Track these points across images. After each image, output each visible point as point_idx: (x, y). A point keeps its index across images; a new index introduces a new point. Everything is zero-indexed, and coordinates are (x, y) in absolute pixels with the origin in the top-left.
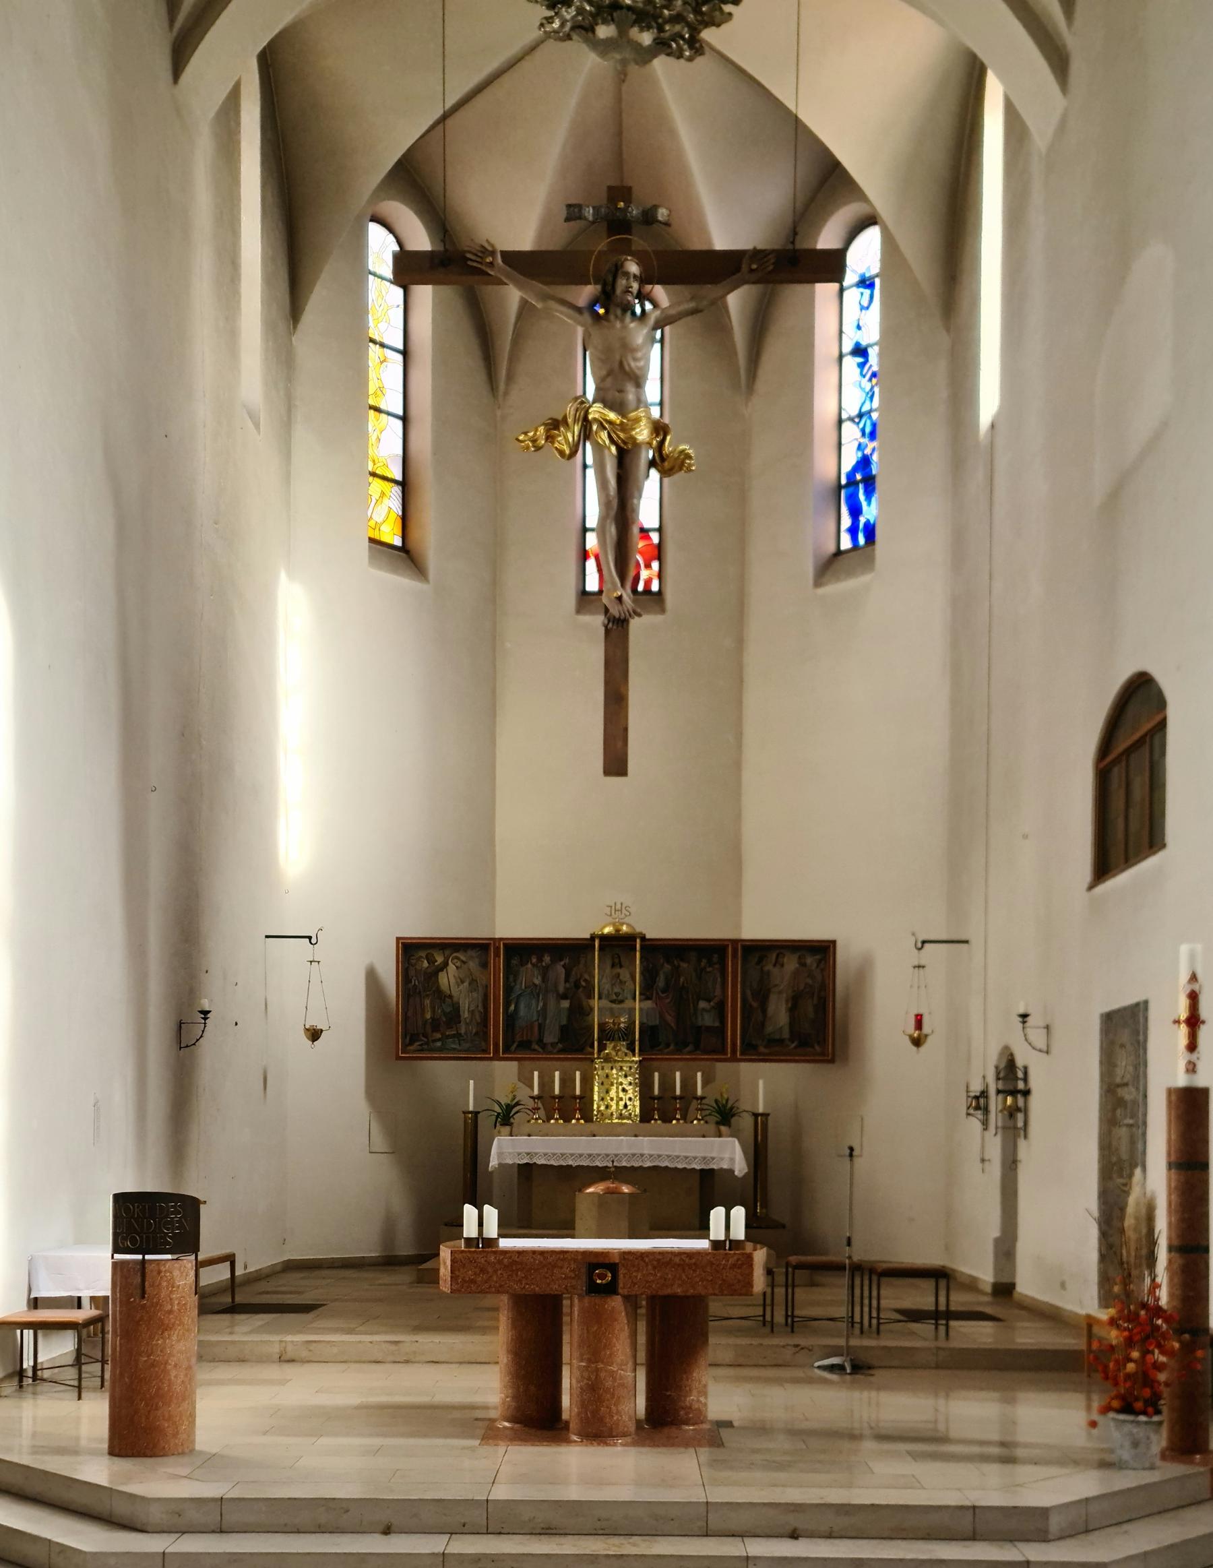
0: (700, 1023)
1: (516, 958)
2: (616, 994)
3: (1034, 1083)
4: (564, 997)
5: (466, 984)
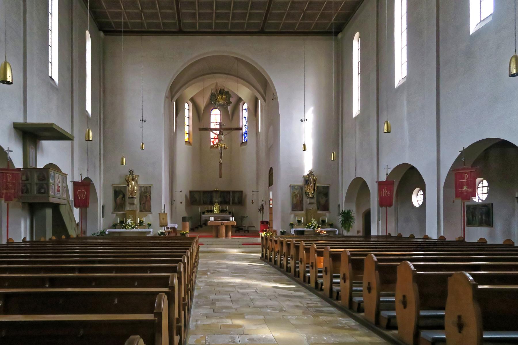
3: (264, 208)
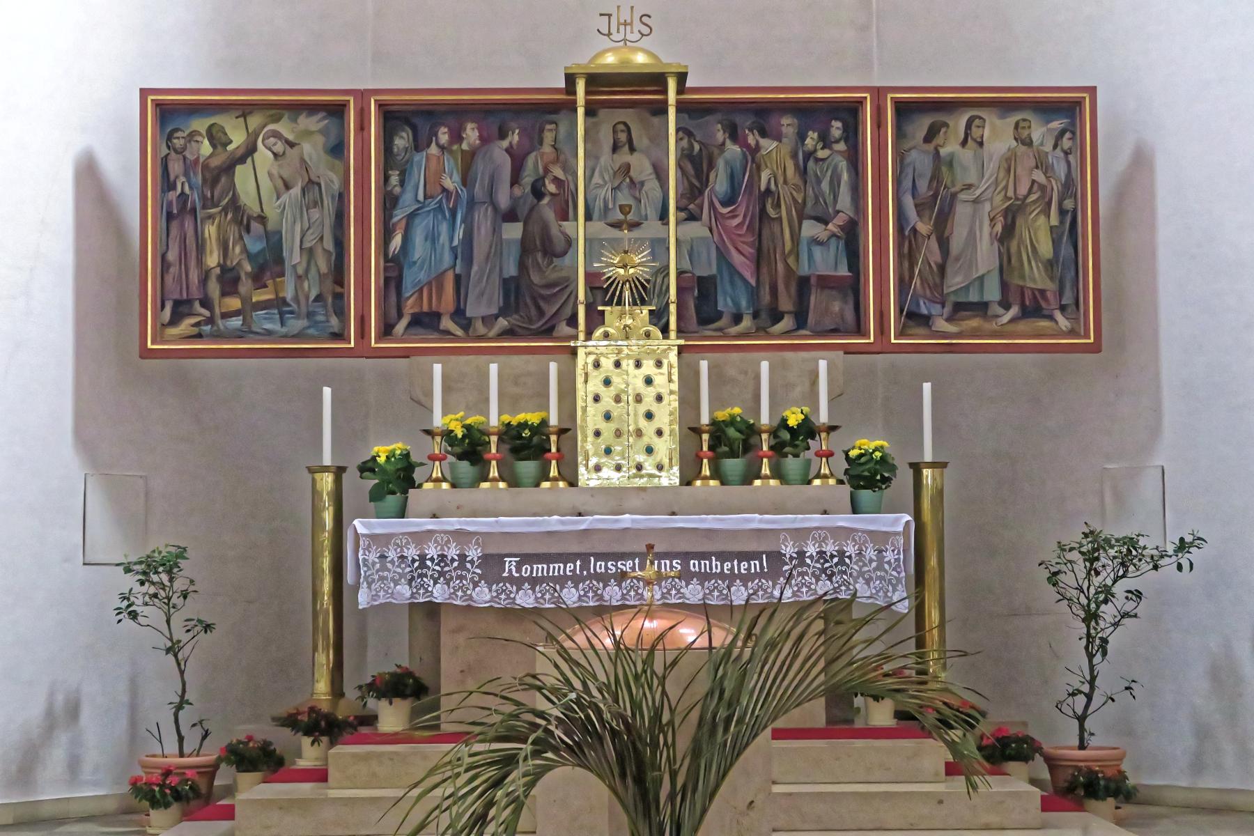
0: (804, 270)
1: (404, 134)
2: (621, 207)
4: (510, 216)
5: (296, 191)
